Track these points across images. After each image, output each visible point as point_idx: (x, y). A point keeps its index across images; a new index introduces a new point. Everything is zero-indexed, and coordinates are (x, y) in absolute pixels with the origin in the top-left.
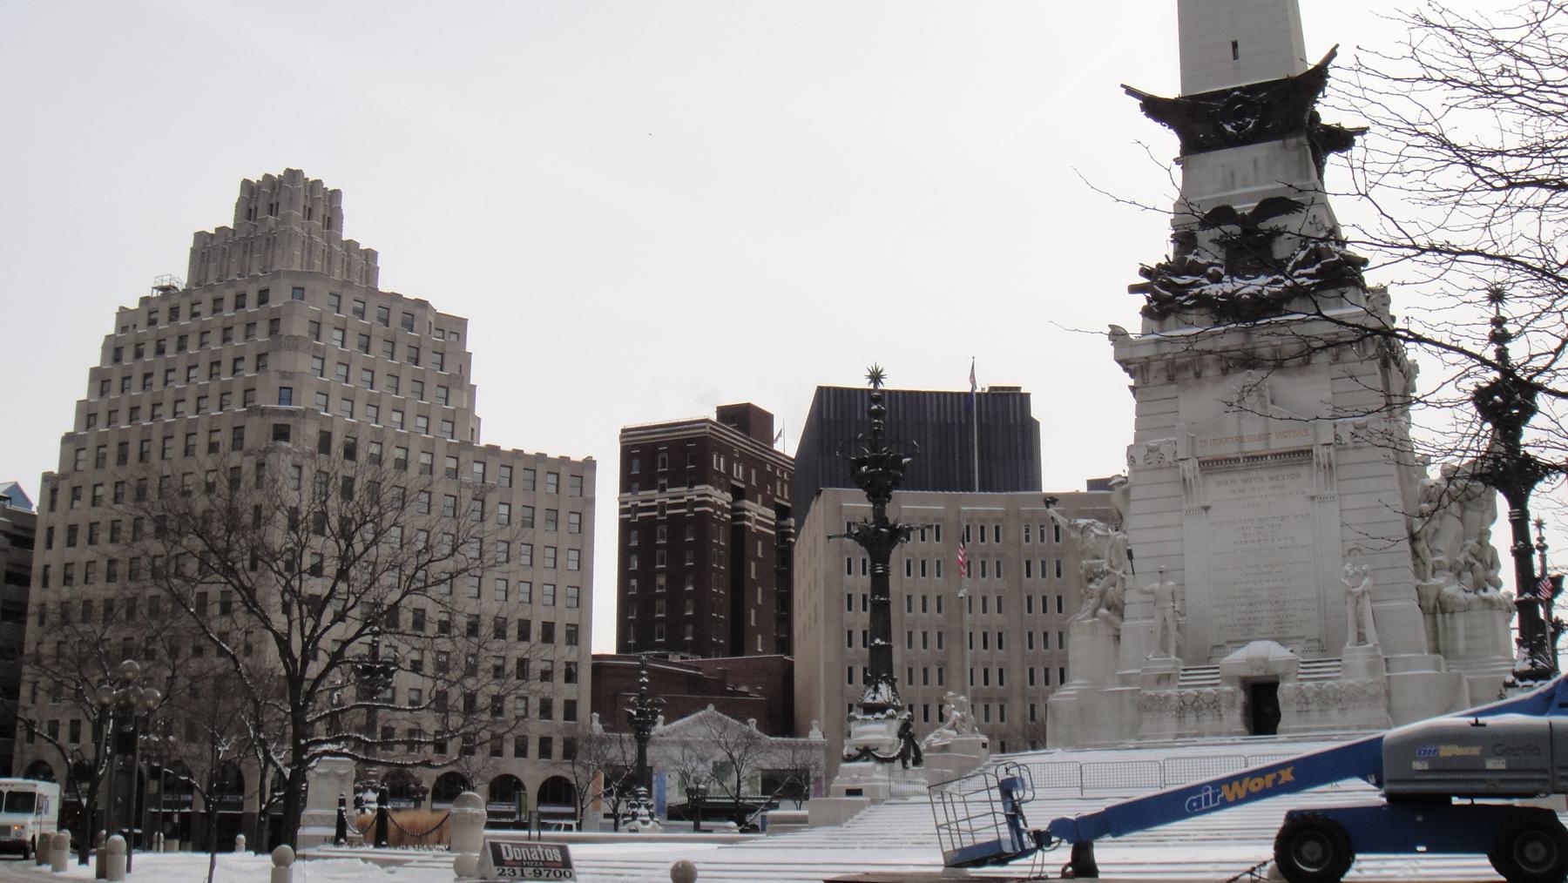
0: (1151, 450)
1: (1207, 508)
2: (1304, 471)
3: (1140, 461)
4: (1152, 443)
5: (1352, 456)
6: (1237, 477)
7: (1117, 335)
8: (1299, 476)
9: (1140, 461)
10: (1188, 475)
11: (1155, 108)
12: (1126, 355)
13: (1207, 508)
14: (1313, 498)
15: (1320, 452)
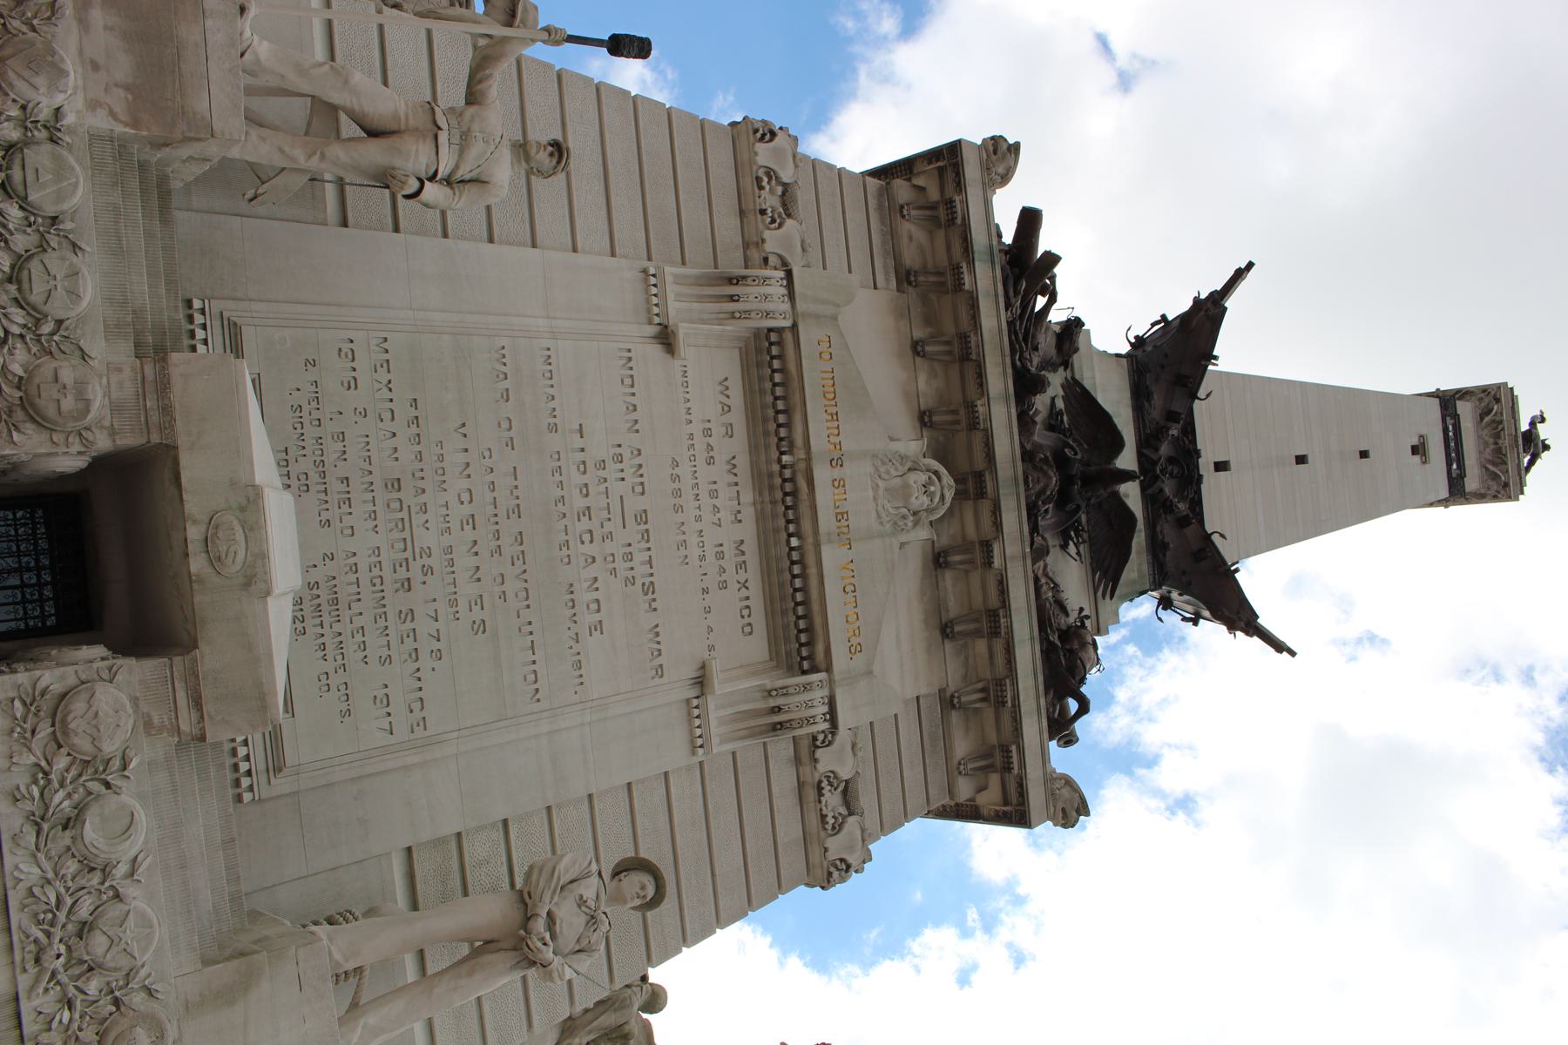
0: (787, 194)
1: (666, 339)
2: (756, 647)
3: (764, 154)
4: (804, 197)
5: (784, 779)
6: (738, 445)
7: (1001, 156)
8: (748, 630)
9: (764, 154)
10: (749, 291)
11: (1206, 315)
12: (972, 171)
13: (666, 339)
14: (701, 682)
15: (808, 698)
